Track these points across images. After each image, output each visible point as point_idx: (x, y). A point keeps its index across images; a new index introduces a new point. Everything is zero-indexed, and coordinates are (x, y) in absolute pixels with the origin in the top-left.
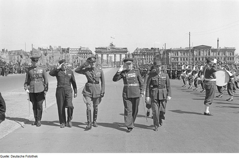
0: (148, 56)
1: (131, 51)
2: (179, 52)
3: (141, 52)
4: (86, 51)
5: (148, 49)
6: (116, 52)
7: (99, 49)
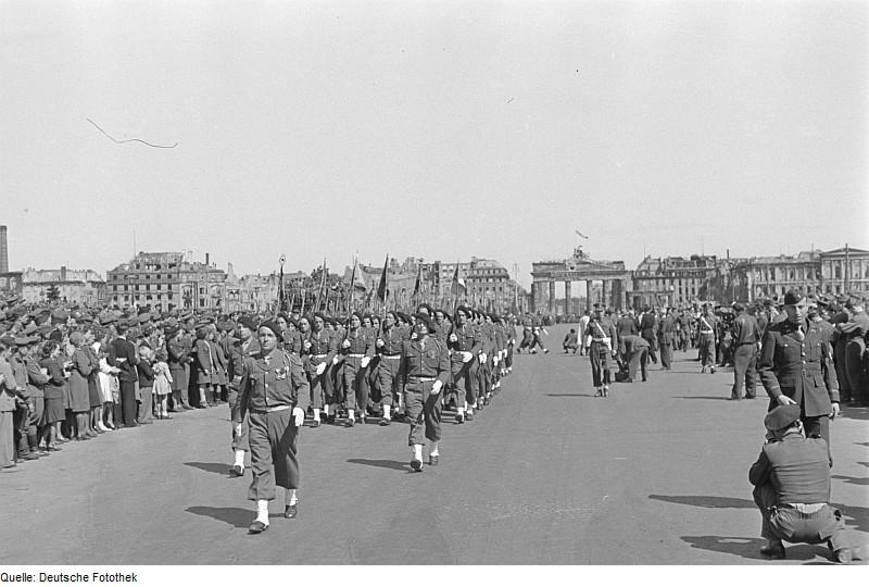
0: (683, 281)
1: (631, 266)
2: (777, 270)
3: (660, 268)
4: (491, 271)
5: (681, 259)
6: (594, 274)
7: (544, 267)
